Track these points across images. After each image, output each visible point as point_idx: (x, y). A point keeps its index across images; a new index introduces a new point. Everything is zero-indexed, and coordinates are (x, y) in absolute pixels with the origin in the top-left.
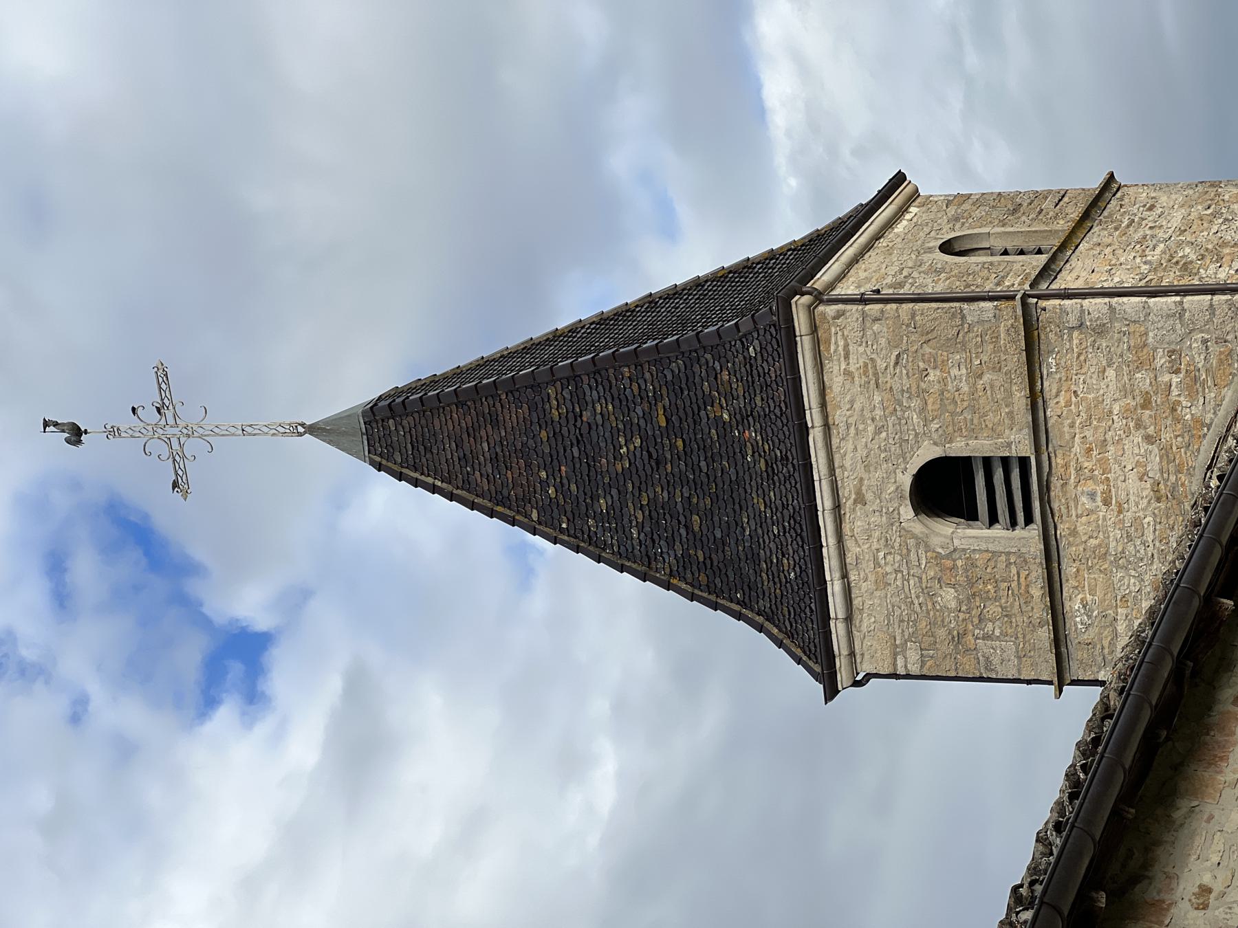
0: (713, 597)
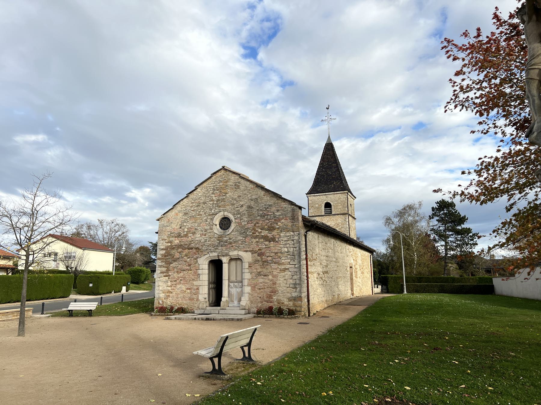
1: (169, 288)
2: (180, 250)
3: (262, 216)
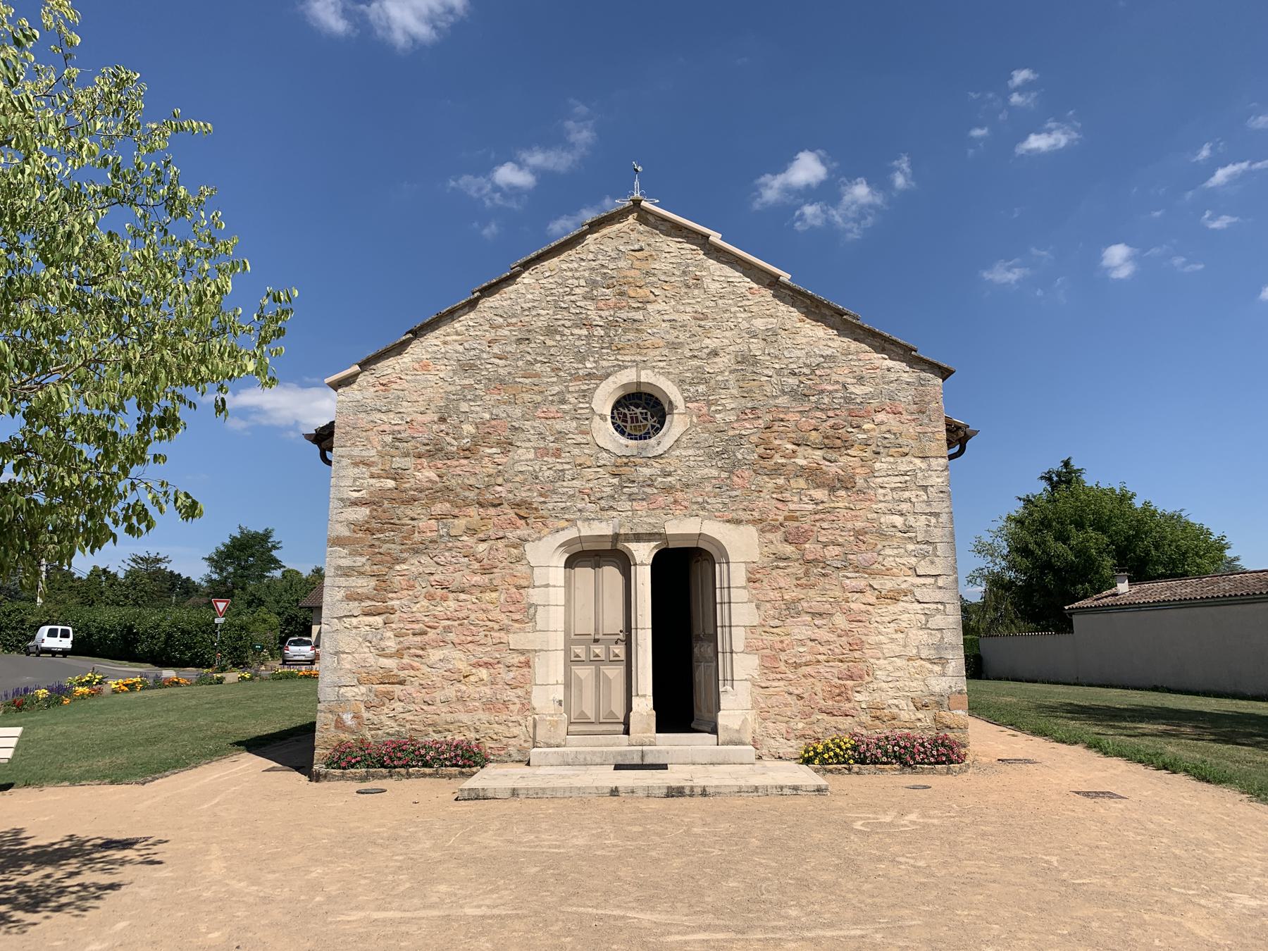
2: (439, 508)
3: (799, 395)
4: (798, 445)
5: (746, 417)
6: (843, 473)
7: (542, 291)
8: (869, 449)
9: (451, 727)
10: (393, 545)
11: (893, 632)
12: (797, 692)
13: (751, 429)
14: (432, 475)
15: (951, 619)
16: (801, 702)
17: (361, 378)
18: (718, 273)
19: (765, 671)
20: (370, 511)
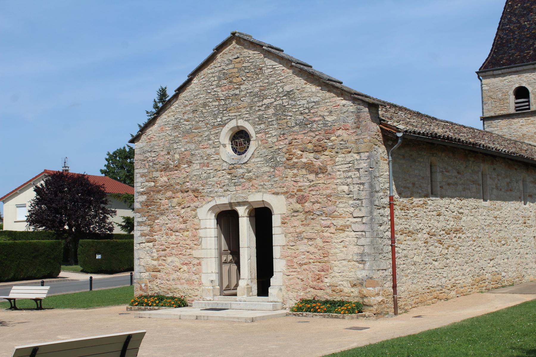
0: (495, 45)
1: (155, 263)
2: (169, 194)
4: (303, 151)
5: (281, 139)
6: (322, 165)
7: (201, 85)
8: (334, 151)
9: (176, 290)
10: (154, 212)
11: (342, 247)
12: (301, 278)
13: (283, 145)
14: (165, 179)
15: (368, 240)
16: (302, 283)
17: (142, 137)
18: (269, 64)
19: (289, 267)
20: (147, 197)
